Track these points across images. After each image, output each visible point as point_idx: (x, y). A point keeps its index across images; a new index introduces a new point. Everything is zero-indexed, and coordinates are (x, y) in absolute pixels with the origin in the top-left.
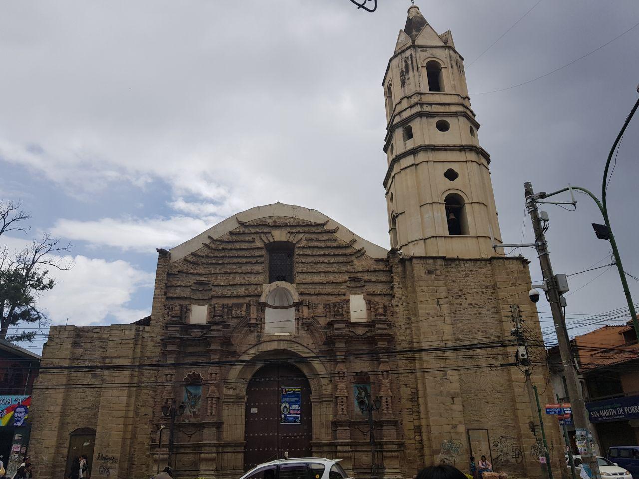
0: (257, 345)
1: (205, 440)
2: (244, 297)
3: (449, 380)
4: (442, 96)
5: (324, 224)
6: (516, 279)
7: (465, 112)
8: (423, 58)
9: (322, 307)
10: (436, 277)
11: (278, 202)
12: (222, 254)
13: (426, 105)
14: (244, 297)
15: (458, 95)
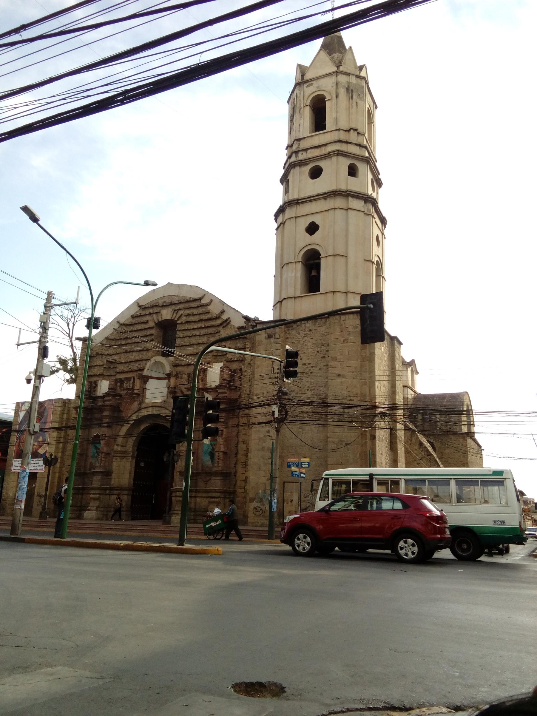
0: (138, 411)
1: (94, 484)
2: (136, 371)
3: (271, 437)
4: (321, 136)
5: (200, 299)
6: (349, 334)
7: (338, 151)
8: (307, 95)
9: (185, 376)
10: (275, 340)
11: (169, 283)
12: (126, 335)
13: (301, 152)
14: (136, 371)
15: (339, 130)
